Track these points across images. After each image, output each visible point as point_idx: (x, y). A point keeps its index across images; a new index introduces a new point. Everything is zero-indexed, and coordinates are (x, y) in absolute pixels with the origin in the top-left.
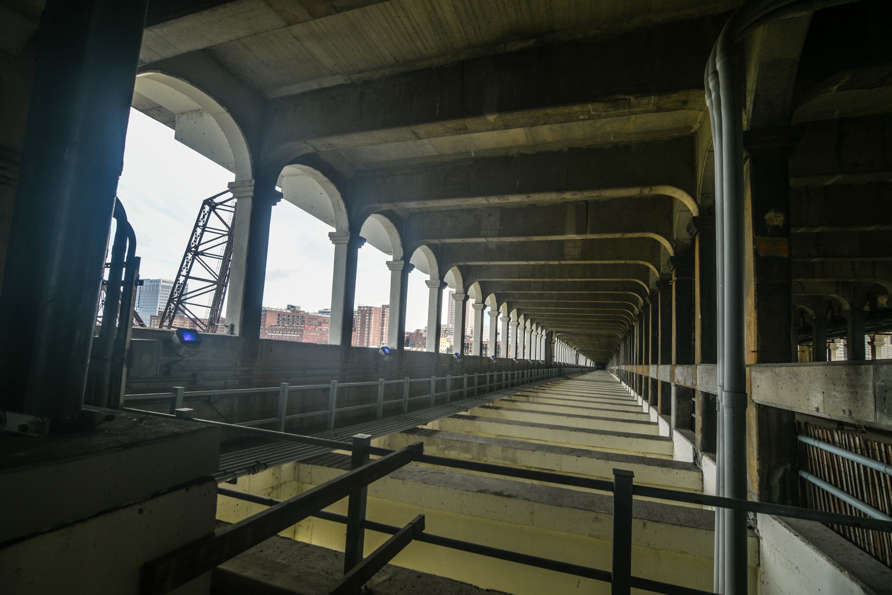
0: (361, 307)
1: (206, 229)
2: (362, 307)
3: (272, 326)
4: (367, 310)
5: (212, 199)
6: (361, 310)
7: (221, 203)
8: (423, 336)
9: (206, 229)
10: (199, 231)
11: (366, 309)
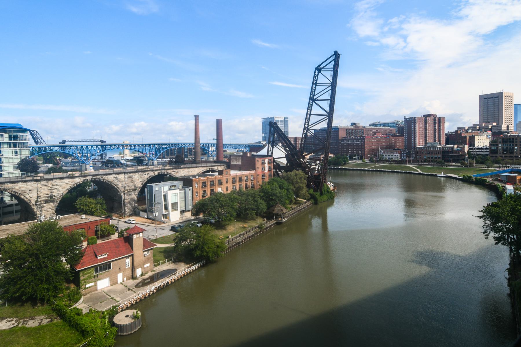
0: (407, 118)
1: (317, 85)
2: (408, 118)
3: (343, 138)
4: (411, 120)
5: (319, 66)
7: (324, 67)
8: (462, 135)
9: (317, 85)
10: (314, 86)
11: (411, 119)
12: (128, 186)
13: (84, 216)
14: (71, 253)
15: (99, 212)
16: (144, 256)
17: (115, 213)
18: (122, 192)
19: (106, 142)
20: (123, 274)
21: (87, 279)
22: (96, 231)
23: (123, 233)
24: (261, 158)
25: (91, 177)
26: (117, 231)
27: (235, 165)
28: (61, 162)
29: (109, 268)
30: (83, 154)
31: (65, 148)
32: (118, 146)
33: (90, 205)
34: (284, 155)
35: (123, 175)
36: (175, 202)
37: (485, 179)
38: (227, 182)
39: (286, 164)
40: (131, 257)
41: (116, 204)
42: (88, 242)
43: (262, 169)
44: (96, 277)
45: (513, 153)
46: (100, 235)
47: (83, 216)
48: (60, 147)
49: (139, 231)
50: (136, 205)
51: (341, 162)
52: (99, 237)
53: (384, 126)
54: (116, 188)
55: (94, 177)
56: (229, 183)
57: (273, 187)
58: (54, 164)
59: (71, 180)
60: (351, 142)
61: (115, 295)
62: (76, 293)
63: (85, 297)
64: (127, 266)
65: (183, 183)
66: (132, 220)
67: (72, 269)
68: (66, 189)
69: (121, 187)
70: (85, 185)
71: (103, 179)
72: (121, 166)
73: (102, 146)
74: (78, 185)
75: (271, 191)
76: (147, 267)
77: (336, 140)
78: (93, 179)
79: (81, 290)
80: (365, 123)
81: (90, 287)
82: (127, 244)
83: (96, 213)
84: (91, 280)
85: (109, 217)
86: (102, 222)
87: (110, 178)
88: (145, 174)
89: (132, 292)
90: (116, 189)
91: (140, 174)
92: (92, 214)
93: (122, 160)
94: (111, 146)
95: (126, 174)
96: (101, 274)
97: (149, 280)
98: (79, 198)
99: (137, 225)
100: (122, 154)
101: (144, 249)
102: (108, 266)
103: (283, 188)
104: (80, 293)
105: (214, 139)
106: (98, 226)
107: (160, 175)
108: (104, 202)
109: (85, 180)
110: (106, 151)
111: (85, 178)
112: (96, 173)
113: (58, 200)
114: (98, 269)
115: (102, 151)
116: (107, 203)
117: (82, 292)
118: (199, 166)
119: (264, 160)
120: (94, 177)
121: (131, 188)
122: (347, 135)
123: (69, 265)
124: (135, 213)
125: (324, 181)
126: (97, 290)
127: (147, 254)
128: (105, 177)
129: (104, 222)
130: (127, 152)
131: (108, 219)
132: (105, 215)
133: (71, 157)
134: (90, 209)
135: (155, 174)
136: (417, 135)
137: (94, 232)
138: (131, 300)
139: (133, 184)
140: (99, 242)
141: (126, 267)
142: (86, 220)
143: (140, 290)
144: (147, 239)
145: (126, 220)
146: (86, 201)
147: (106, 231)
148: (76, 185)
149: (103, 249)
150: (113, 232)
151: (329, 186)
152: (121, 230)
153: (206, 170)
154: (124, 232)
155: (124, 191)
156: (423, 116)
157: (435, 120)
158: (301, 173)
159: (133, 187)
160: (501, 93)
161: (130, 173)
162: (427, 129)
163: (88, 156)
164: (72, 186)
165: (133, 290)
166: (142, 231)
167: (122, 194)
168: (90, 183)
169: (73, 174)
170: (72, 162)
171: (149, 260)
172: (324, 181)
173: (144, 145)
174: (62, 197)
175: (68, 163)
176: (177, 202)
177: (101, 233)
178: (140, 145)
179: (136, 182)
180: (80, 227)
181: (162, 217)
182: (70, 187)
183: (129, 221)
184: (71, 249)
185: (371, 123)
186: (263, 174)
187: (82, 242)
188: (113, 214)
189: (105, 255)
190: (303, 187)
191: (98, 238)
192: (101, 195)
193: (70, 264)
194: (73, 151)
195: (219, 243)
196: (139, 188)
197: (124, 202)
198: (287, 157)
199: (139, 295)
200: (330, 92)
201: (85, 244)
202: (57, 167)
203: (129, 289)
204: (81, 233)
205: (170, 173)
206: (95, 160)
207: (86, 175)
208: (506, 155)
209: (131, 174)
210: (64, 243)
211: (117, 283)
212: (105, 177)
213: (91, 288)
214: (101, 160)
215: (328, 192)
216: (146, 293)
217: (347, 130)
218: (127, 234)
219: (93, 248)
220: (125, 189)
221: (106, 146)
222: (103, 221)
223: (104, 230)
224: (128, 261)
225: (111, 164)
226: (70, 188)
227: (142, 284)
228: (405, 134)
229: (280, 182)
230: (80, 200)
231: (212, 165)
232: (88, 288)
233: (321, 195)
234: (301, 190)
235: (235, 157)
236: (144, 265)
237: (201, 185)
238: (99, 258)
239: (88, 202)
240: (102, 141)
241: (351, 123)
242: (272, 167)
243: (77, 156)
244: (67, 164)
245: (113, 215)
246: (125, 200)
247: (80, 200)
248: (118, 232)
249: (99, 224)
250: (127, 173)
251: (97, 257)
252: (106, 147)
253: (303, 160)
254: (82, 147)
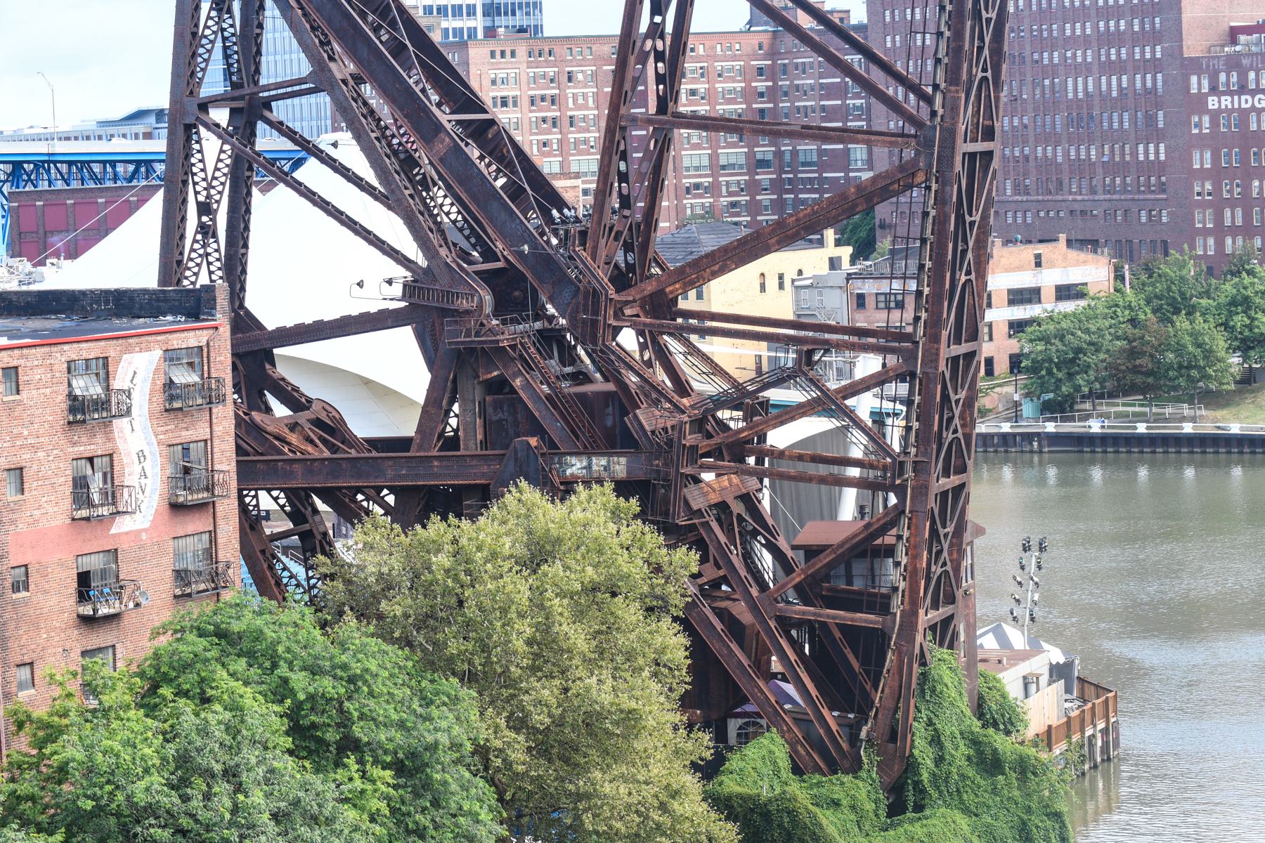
3: (1233, 34)
24: (53, 340)
39: (422, 402)
43: (80, 484)
51: (1208, 354)
57: (204, 731)
75: (170, 800)
77: (1154, 66)
103: (350, 745)
119: (103, 370)
125: (927, 617)
151: (1011, 681)
158: (603, 528)
172: (927, 617)
186: (94, 563)
190: (630, 720)
215: (990, 763)
229: (314, 670)
233: (896, 809)
234: (611, 755)
242: (225, 461)
253: (651, 339)
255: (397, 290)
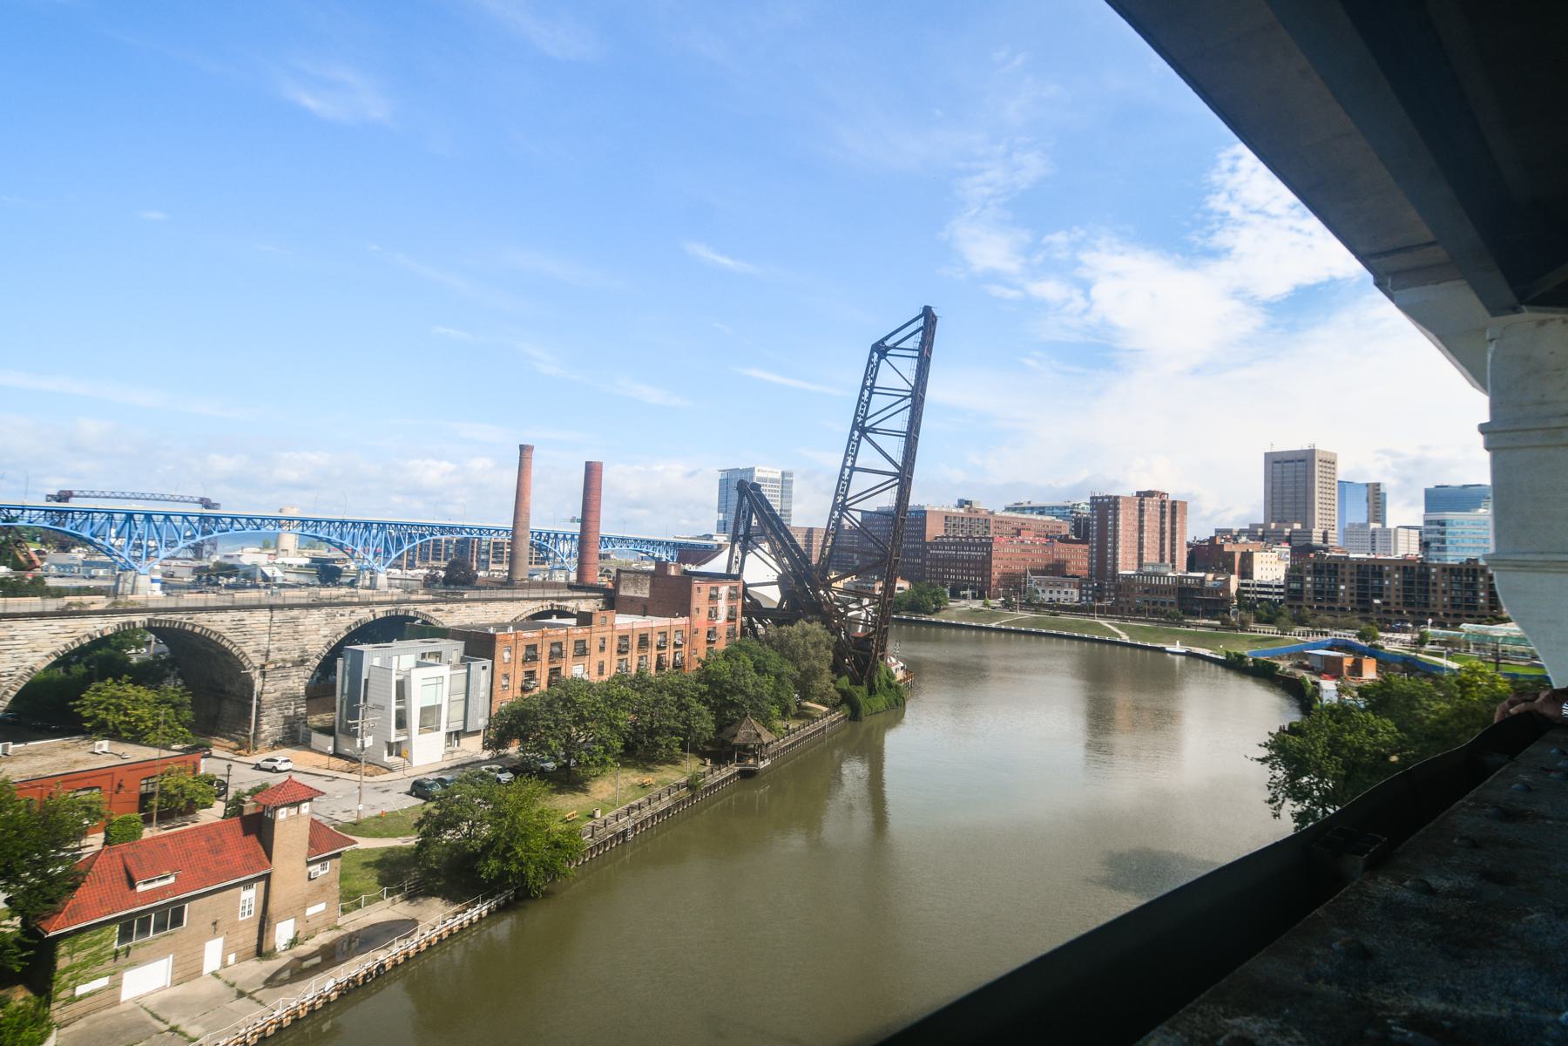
0: (1097, 498)
1: (875, 390)
3: (936, 538)
4: (1109, 503)
5: (882, 341)
6: (1097, 503)
7: (895, 346)
8: (1226, 549)
9: (875, 390)
10: (866, 393)
11: (1106, 500)
12: (280, 650)
13: (105, 745)
14: (33, 875)
15: (164, 733)
16: (310, 879)
17: (224, 737)
18: (256, 668)
19: (217, 504)
20: (225, 942)
21: (84, 966)
22: (145, 798)
23: (244, 802)
24: (708, 582)
25: (151, 616)
26: (223, 798)
27: (632, 599)
28: (42, 560)
29: (177, 921)
30: (130, 538)
31: (66, 517)
32: (259, 521)
33: (135, 709)
34: (773, 577)
35: (267, 612)
36: (433, 704)
37: (1275, 662)
38: (602, 649)
39: (778, 602)
40: (262, 884)
41: (229, 708)
42: (107, 834)
43: (710, 613)
44: (122, 958)
45: (1335, 601)
46: (155, 811)
47: (100, 746)
48: (46, 511)
49: (298, 796)
50: (302, 710)
52: (152, 815)
53: (1041, 513)
54: (236, 654)
55: (162, 617)
56: (607, 651)
57: (738, 666)
58: (17, 566)
59: (72, 623)
60: (956, 550)
61: (184, 1016)
62: (29, 1020)
63: (64, 1031)
64: (243, 914)
65: (466, 645)
66: (281, 759)
67: (29, 929)
68: (47, 651)
69: (254, 652)
70: (124, 640)
71: (190, 624)
72: (263, 584)
73: (203, 518)
74: (98, 640)
75: (731, 680)
76: (316, 916)
77: (919, 543)
78: (156, 621)
79: (54, 1006)
80: (992, 503)
81: (91, 994)
82: (253, 838)
83: (152, 736)
84: (101, 967)
85: (201, 749)
86: (169, 767)
87: (219, 624)
88: (341, 612)
89: (253, 1004)
90: (236, 657)
91: (324, 611)
92: (137, 738)
93: (269, 565)
94: (234, 519)
95: (276, 612)
96: (143, 945)
97: (318, 960)
98: (96, 685)
99: (296, 777)
100: (273, 546)
101: (309, 856)
102: (172, 916)
103: (766, 671)
104: (46, 1017)
105: (573, 520)
106: (154, 780)
107: (391, 617)
108: (188, 700)
109: (124, 624)
110: (216, 534)
111: (125, 619)
112: (171, 603)
113: (11, 689)
114: (130, 927)
115: (203, 534)
116: (195, 706)
117: (57, 1012)
118: (520, 596)
119: (717, 589)
120: (162, 617)
121: (288, 656)
122: (946, 530)
123: (17, 921)
124: (294, 736)
125: (879, 654)
126: (117, 1003)
127: (321, 873)
128: (201, 619)
129: (176, 767)
130: (289, 540)
131: (195, 757)
132: (186, 741)
133: (84, 546)
134: (130, 722)
135: (374, 615)
136: (1120, 543)
137: (137, 799)
138: (243, 1031)
139: (295, 642)
140: (147, 833)
141: (241, 919)
142: (111, 759)
143: (281, 995)
144: (324, 821)
145: (258, 758)
146: (119, 694)
147: (183, 796)
148: (87, 640)
149: (159, 860)
150: (206, 800)
151: (893, 669)
152: (237, 793)
153: (541, 610)
154: (247, 799)
155: (263, 666)
156: (1135, 494)
157: (1163, 507)
158: (818, 630)
159: (296, 655)
160: (1312, 452)
161: (291, 607)
162: (1145, 528)
163: (148, 547)
164: (73, 643)
165: (255, 995)
166: (311, 795)
167: (256, 674)
168: (143, 637)
169: (81, 604)
170: (85, 564)
171: (323, 891)
172: (879, 654)
173: (350, 524)
174: (28, 679)
175: (71, 566)
176: (439, 706)
177: (161, 803)
178: (337, 524)
179: (307, 638)
180: (85, 783)
181: (386, 752)
182: (66, 646)
183: (270, 765)
184: (37, 862)
185: (1010, 503)
186: (711, 629)
187: (84, 833)
188: (215, 741)
189: (167, 877)
190: (822, 671)
191: (147, 821)
192: (180, 675)
193: (21, 913)
194: (95, 528)
195: (562, 833)
196: (317, 657)
197: (259, 699)
198: (782, 582)
199: (277, 1013)
200: (907, 412)
201: (95, 841)
202: (23, 578)
203: (241, 994)
204: (83, 802)
205: (426, 615)
206: (174, 563)
207: (130, 607)
208: (1320, 604)
209: (295, 612)
210: (9, 840)
211: (199, 973)
212: (201, 619)
213: (97, 997)
214: (196, 564)
215: (890, 686)
216: (303, 1004)
217: (946, 517)
218: (257, 807)
219: (122, 855)
220: (267, 660)
221: (217, 518)
222: (177, 763)
223: (174, 792)
224: (250, 897)
225: (228, 576)
226: (63, 648)
227: (291, 975)
228: (1092, 537)
229: (759, 655)
230: (98, 690)
231: (561, 595)
232: (81, 997)
233: (870, 694)
234: (816, 678)
235: (633, 576)
236: (305, 908)
237: (521, 653)
238: (141, 888)
239: (127, 698)
240: (206, 503)
241: (960, 501)
242: (739, 610)
243: (106, 543)
244: (65, 571)
245: (214, 742)
246: (264, 696)
247: (98, 690)
248: (226, 801)
249: (158, 771)
250: (281, 607)
251: (132, 885)
252: (217, 523)
253: (826, 593)
254: (130, 516)
255: (776, 578)
